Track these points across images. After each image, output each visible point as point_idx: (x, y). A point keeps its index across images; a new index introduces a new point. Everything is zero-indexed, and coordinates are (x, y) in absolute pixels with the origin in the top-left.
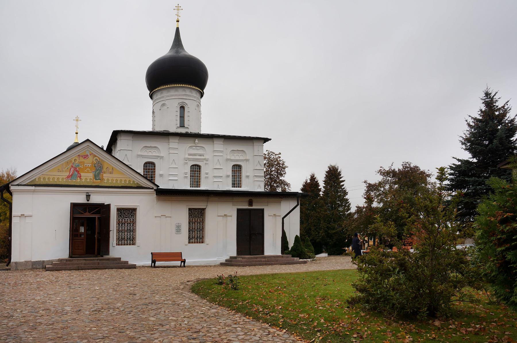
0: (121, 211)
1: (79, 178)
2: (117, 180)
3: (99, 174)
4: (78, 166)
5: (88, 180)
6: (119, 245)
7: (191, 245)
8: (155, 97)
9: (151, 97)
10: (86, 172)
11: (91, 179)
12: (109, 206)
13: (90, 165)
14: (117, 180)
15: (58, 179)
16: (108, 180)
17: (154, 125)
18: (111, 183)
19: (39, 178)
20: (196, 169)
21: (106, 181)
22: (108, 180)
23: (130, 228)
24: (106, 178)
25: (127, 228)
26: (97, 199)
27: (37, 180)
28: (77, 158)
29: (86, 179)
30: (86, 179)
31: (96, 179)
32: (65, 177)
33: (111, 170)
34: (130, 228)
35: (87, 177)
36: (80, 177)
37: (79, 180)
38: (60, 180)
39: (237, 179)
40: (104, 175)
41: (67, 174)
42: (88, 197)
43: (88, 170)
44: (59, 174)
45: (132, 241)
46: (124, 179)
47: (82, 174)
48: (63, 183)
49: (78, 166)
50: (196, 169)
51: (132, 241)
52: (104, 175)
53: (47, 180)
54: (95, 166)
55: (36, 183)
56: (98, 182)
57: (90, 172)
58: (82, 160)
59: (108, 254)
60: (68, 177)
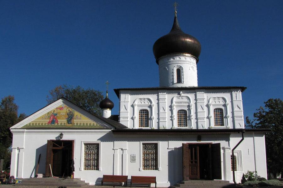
1: (56, 123)
3: (71, 119)
4: (56, 115)
5: (63, 124)
10: (61, 119)
11: (65, 123)
13: (64, 114)
16: (77, 124)
18: (79, 126)
19: (30, 124)
21: (76, 125)
22: (77, 124)
24: (75, 123)
26: (67, 137)
28: (56, 110)
30: (61, 123)
31: (68, 124)
32: (46, 123)
35: (62, 121)
36: (57, 122)
37: (56, 124)
38: (44, 125)
40: (75, 120)
41: (48, 120)
42: (61, 135)
43: (63, 118)
44: (43, 120)
47: (59, 120)
54: (68, 115)
57: (64, 119)
58: (59, 110)
60: (49, 122)
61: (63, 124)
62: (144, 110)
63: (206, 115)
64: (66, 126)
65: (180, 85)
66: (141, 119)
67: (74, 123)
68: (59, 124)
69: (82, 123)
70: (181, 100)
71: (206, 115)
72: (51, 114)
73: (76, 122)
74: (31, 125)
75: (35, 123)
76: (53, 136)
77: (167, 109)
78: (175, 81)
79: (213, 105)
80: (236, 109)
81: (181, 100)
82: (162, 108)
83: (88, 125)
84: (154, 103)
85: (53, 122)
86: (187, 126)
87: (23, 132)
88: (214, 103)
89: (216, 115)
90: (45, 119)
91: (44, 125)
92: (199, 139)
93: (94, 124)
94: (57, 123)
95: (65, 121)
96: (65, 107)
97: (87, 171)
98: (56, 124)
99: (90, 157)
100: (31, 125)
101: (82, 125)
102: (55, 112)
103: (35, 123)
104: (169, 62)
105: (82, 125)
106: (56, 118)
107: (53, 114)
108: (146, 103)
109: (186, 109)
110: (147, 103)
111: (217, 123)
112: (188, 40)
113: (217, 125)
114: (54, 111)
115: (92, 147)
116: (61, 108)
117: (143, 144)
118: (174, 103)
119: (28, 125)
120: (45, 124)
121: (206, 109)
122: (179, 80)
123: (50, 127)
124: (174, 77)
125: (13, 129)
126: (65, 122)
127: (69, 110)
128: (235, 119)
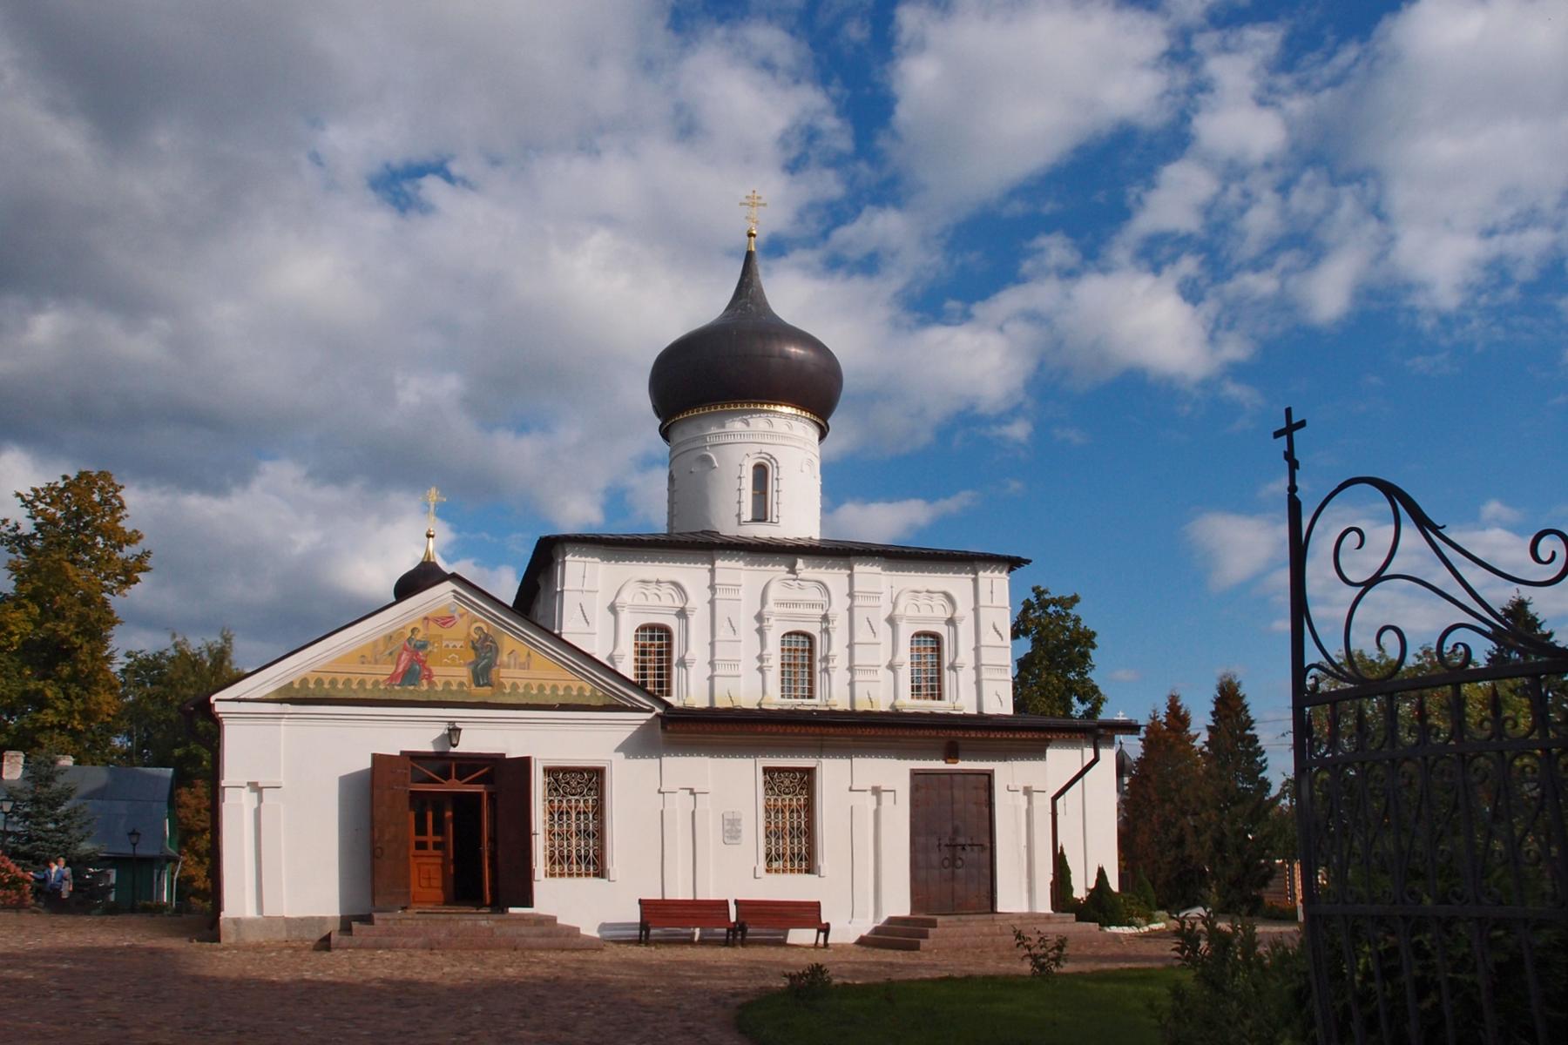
0: (554, 773)
2: (541, 688)
3: (488, 668)
4: (424, 646)
5: (454, 687)
6: (552, 875)
7: (773, 876)
8: (677, 437)
9: (665, 433)
10: (447, 665)
11: (461, 684)
12: (524, 764)
14: (541, 688)
15: (362, 683)
16: (515, 686)
17: (670, 524)
18: (524, 695)
19: (304, 681)
20: (802, 654)
22: (515, 686)
23: (587, 825)
24: (507, 683)
25: (578, 826)
27: (296, 686)
29: (448, 684)
30: (448, 684)
31: (478, 685)
33: (523, 659)
34: (587, 825)
35: (452, 673)
36: (430, 677)
38: (369, 687)
39: (931, 683)
40: (503, 672)
41: (390, 669)
42: (453, 733)
43: (453, 659)
44: (365, 668)
45: (596, 865)
46: (565, 684)
47: (436, 670)
48: (376, 696)
49: (424, 646)
50: (802, 654)
51: (596, 865)
52: (503, 672)
53: (326, 686)
54: (474, 648)
55: (294, 695)
56: (484, 693)
58: (435, 629)
59: (530, 904)
60: (392, 677)
61: (454, 687)
62: (652, 627)
63: (884, 659)
64: (469, 694)
65: (762, 532)
66: (643, 661)
67: (502, 685)
68: (440, 688)
69: (535, 684)
70: (795, 594)
71: (884, 657)
72: (403, 641)
73: (444, 679)
74: (312, 686)
75: (327, 679)
76: (415, 734)
77: (747, 625)
78: (747, 514)
79: (911, 620)
80: (988, 637)
81: (795, 594)
82: (726, 623)
83: (521, 690)
84: (698, 600)
85: (410, 675)
86: (810, 697)
87: (278, 716)
88: (912, 612)
89: (916, 655)
90: (376, 662)
91: (369, 687)
92: (952, 754)
93: (581, 688)
94: (431, 683)
95: (462, 674)
96: (461, 616)
97: (558, 881)
98: (425, 686)
99: (561, 826)
100: (312, 686)
101: (535, 692)
102: (419, 636)
103: (327, 679)
104: (727, 434)
105: (535, 692)
106: (424, 662)
107: (409, 640)
108: (667, 601)
109: (814, 629)
110: (670, 600)
111: (919, 688)
112: (794, 350)
113: (919, 696)
114: (413, 630)
115: (573, 784)
116: (446, 621)
117: (766, 770)
118: (771, 606)
119: (296, 686)
120: (376, 683)
121: (884, 630)
122: (761, 515)
123: (397, 697)
124: (743, 498)
125: (221, 703)
126: (465, 680)
127: (480, 628)
128: (985, 674)
